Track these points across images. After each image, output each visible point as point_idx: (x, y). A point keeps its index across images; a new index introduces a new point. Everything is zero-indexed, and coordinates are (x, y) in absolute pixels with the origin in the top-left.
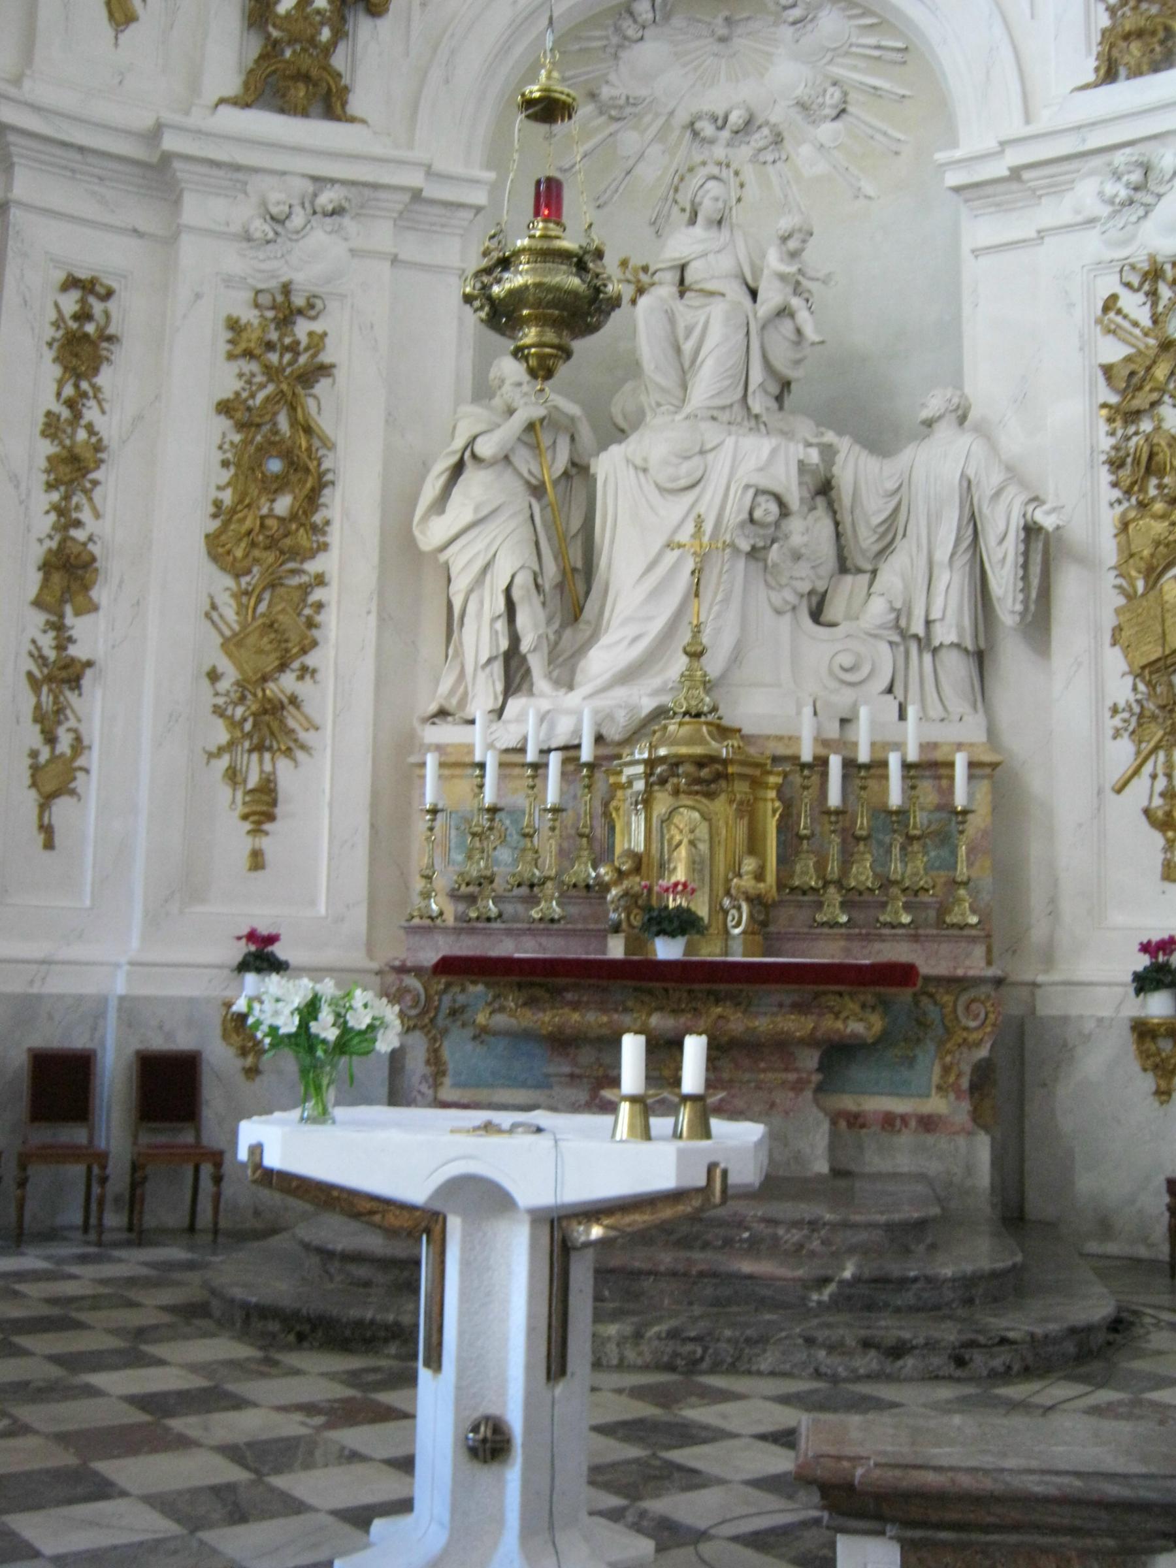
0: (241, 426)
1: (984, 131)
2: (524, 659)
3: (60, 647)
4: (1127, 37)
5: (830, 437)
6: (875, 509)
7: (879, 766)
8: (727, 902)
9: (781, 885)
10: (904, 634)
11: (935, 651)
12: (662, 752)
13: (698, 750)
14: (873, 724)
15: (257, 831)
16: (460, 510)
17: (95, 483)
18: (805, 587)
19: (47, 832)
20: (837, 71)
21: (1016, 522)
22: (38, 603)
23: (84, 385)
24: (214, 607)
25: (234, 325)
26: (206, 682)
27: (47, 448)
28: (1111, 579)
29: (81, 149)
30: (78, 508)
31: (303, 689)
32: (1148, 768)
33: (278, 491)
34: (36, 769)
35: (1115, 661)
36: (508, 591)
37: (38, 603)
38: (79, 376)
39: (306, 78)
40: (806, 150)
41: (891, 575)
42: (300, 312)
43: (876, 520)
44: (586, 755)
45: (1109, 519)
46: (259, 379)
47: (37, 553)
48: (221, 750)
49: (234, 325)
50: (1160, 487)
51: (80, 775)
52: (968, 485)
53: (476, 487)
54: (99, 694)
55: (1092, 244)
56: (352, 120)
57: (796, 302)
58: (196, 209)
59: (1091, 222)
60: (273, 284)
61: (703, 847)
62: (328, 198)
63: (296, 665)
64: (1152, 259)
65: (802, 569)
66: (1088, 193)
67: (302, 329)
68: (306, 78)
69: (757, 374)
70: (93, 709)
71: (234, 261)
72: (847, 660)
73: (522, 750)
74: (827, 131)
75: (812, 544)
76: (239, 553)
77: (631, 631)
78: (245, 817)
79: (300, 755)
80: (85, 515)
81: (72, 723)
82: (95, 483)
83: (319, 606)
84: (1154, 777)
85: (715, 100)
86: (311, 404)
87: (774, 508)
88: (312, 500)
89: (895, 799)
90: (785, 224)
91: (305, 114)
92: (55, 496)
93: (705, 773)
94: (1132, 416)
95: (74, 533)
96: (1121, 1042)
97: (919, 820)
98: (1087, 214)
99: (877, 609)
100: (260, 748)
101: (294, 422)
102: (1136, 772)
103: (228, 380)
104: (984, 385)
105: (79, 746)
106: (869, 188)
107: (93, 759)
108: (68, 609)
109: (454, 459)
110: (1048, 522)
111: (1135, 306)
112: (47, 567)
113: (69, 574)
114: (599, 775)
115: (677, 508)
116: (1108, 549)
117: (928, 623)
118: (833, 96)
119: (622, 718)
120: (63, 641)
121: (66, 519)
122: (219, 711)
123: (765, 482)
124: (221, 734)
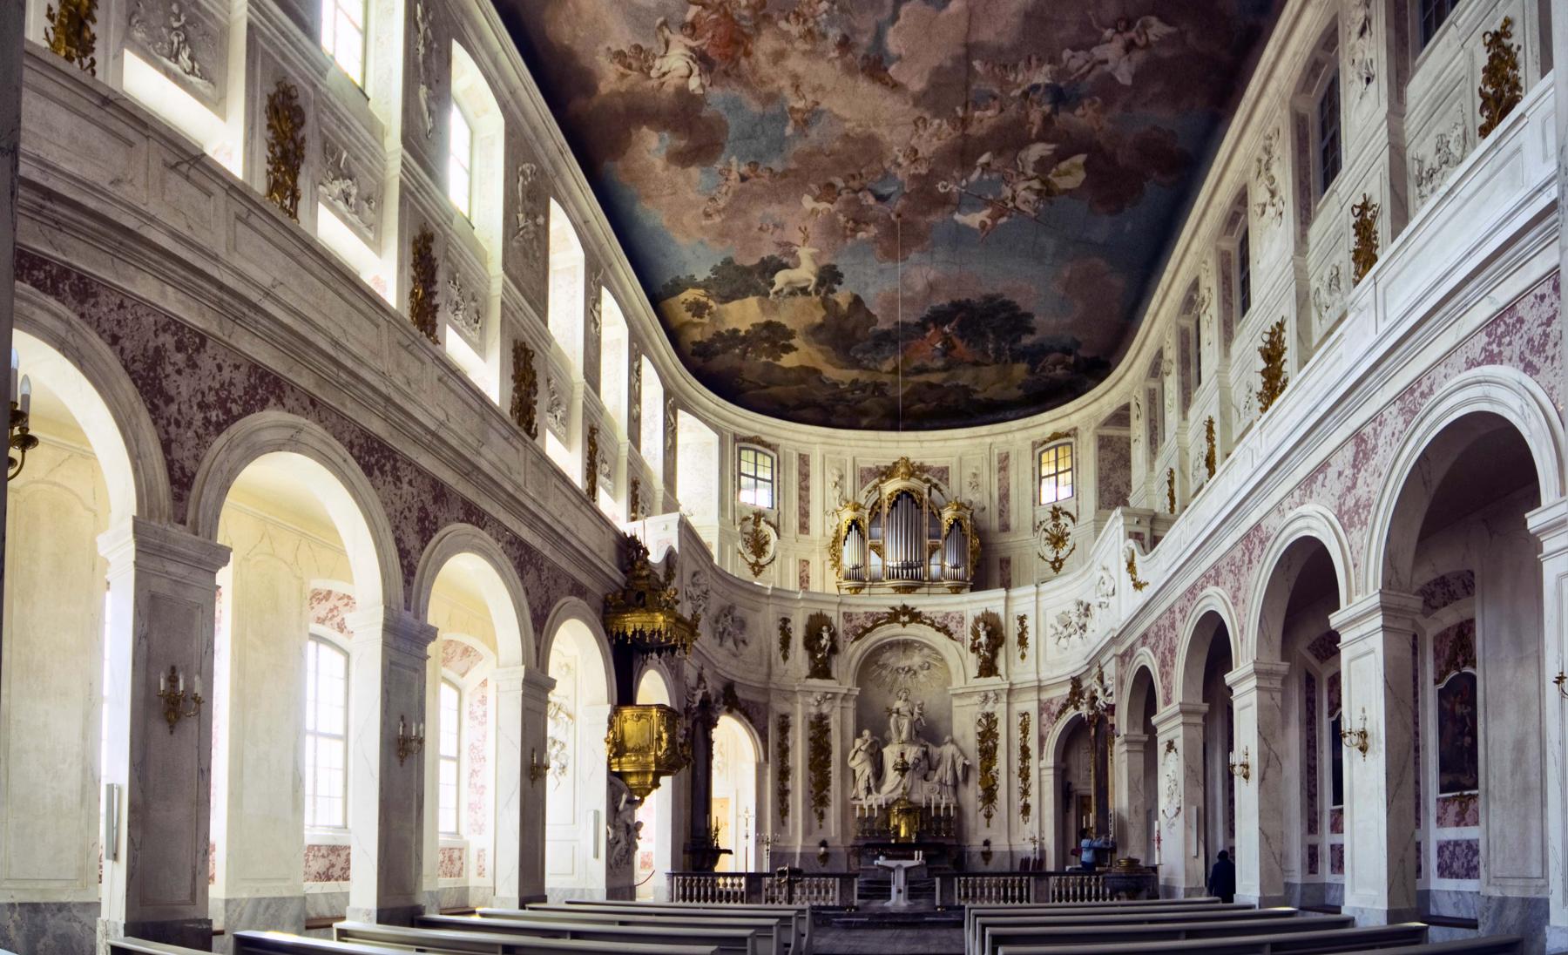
6: (936, 758)
53: (860, 755)
85: (901, 664)
104: (957, 733)
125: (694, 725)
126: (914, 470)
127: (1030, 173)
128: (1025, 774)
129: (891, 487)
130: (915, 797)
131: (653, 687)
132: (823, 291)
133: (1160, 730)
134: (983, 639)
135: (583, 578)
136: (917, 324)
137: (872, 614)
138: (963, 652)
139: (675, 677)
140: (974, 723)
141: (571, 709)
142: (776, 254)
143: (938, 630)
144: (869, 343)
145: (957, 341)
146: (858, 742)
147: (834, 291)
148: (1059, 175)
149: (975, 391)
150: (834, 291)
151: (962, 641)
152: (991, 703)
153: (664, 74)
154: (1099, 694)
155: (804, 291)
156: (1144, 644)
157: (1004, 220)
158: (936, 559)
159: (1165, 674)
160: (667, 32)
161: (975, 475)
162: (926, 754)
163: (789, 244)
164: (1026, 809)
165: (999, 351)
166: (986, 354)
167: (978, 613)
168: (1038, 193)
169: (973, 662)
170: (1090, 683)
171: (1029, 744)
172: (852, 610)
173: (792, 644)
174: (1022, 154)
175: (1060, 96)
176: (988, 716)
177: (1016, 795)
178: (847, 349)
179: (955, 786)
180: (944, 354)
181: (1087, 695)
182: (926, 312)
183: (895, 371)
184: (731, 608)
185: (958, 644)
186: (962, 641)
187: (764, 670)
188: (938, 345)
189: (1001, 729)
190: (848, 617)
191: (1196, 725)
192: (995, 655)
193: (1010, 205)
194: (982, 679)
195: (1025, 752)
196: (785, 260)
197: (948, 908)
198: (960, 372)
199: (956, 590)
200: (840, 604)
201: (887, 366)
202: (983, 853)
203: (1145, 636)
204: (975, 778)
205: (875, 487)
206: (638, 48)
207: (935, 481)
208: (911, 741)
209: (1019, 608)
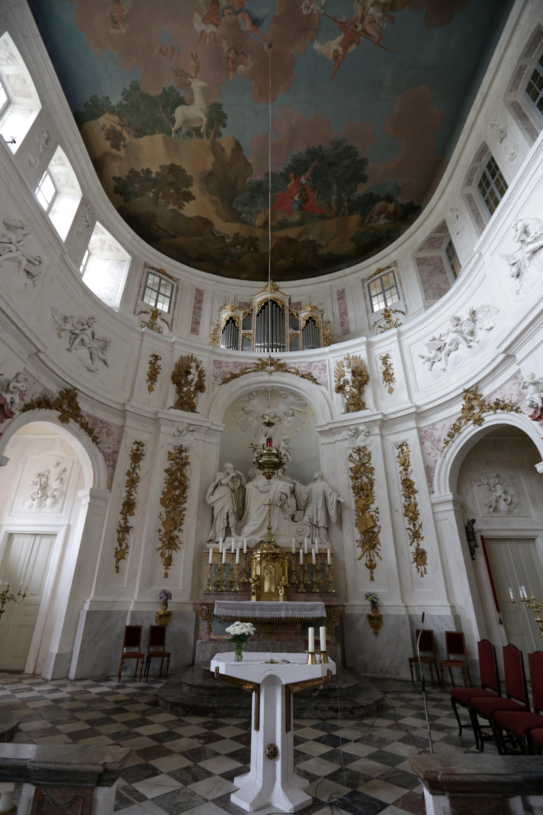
0: (169, 475)
1: (323, 420)
2: (230, 528)
3: (125, 523)
4: (351, 404)
5: (294, 481)
7: (310, 554)
8: (279, 587)
9: (289, 582)
10: (311, 524)
11: (319, 528)
12: (264, 552)
13: (272, 551)
14: (308, 545)
15: (167, 568)
17: (137, 486)
18: (291, 514)
19: (117, 568)
21: (335, 500)
22: (121, 513)
23: (136, 465)
24: (161, 515)
25: (170, 453)
26: (158, 532)
27: (127, 478)
28: (354, 512)
29: (141, 415)
30: (132, 492)
31: (180, 534)
32: (365, 554)
33: (177, 489)
34: (116, 553)
35: (356, 530)
36: (227, 514)
37: (121, 513)
38: (135, 463)
39: (188, 404)
40: (286, 422)
41: (309, 511)
42: (184, 451)
43: (304, 499)
44: (245, 551)
45: (353, 500)
46: (174, 465)
47: (122, 501)
48: (160, 548)
49: (170, 453)
50: (363, 493)
51: (127, 554)
52: (324, 492)
54: (133, 534)
55: (346, 444)
56: (197, 412)
57: (287, 453)
58: (163, 429)
59: (346, 439)
60: (178, 445)
61: (274, 574)
62: (191, 428)
63: (178, 529)
64: (359, 447)
65: (290, 510)
66: (345, 434)
67: (184, 454)
68: (188, 404)
70: (131, 538)
71: (171, 440)
72: (300, 530)
73: (230, 550)
74: (290, 418)
75: (295, 505)
76: (167, 503)
77: (254, 523)
78: (164, 565)
79: (178, 550)
80: (134, 493)
81: (126, 541)
82: (137, 486)
83: (184, 515)
84: (367, 556)
86: (185, 470)
87: (285, 497)
88: (184, 492)
89: (314, 562)
90: (285, 437)
91: (187, 411)
92: (128, 489)
93: (274, 557)
94: (357, 479)
95: (131, 497)
97: (318, 567)
98: (345, 438)
99: (306, 519)
101: (181, 474)
102: (363, 555)
103: (167, 465)
105: (127, 547)
106: (298, 430)
107: (130, 550)
108: (128, 514)
109: (216, 484)
110: (342, 501)
111: (355, 456)
112: (124, 505)
113: (129, 506)
114: (248, 556)
115: (264, 496)
116: (353, 506)
117: (317, 522)
118: (291, 412)
119: (253, 543)
120: (126, 522)
121: (129, 494)
122: (160, 539)
123: (283, 491)
124: (160, 545)
128: (411, 512)
134: (348, 376)
137: (240, 364)
138: (328, 394)
143: (303, 376)
152: (362, 437)
164: (420, 556)
169: (338, 401)
171: (412, 478)
172: (223, 359)
173: (159, 378)
176: (359, 450)
185: (323, 388)
189: (376, 462)
190: (218, 364)
192: (361, 392)
195: (408, 486)
204: (350, 518)
209: (379, 351)
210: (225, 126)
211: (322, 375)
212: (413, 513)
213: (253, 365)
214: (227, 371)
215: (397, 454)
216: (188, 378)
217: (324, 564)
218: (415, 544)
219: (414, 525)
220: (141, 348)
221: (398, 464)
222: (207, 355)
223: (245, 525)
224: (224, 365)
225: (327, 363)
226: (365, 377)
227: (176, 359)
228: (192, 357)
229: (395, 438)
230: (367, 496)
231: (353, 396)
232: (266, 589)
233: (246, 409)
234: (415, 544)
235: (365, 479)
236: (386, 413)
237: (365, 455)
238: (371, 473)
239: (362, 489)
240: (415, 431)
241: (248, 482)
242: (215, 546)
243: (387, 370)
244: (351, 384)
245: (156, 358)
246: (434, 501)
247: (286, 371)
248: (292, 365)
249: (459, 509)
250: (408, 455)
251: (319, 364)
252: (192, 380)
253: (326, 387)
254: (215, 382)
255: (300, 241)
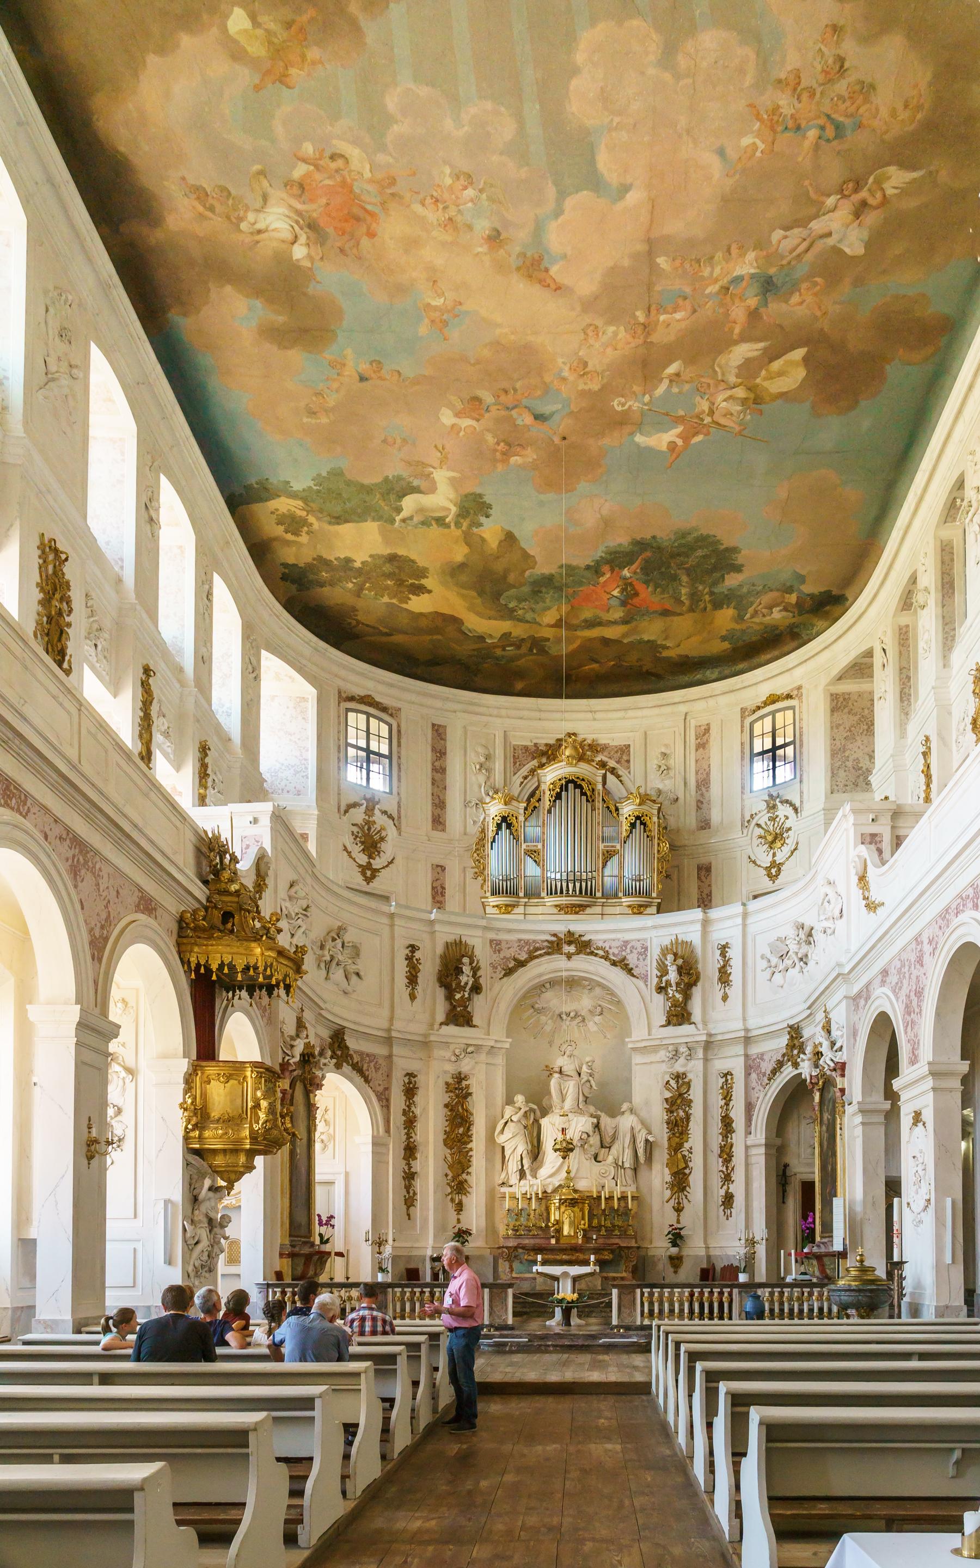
0: (451, 1110)
5: (599, 1113)
16: (508, 1133)
20: (600, 1003)
25: (447, 1083)
35: (667, 1171)
40: (591, 1023)
45: (666, 1136)
49: (447, 1083)
52: (632, 1128)
53: (511, 1129)
56: (474, 1026)
58: (438, 1053)
62: (470, 1050)
65: (593, 1149)
66: (662, 1055)
67: (464, 1083)
68: (463, 1016)
69: (581, 1098)
74: (597, 1019)
80: (413, 1135)
85: (565, 1009)
88: (469, 1129)
90: (588, 1059)
94: (672, 1112)
96: (667, 1261)
99: (610, 1159)
100: (458, 1193)
110: (651, 1139)
118: (599, 1009)
125: (292, 1085)
126: (586, 751)
127: (732, 379)
128: (726, 1154)
129: (552, 774)
130: (582, 1185)
131: (241, 1037)
132: (465, 524)
133: (903, 1097)
134: (673, 976)
135: (150, 887)
136: (588, 568)
137: (527, 942)
139: (267, 1024)
140: (661, 1084)
141: (130, 1063)
142: (405, 474)
143: (614, 964)
144: (526, 589)
145: (640, 587)
146: (509, 1111)
147: (481, 525)
148: (770, 378)
149: (665, 648)
150: (481, 525)
151: (645, 978)
152: (682, 1060)
153: (259, 232)
154: (825, 1049)
155: (440, 521)
156: (883, 983)
157: (699, 438)
158: (612, 868)
159: (911, 1025)
160: (265, 183)
161: (664, 755)
162: (597, 1126)
163: (424, 465)
164: (728, 1200)
165: (695, 597)
166: (679, 601)
167: (666, 942)
168: (744, 402)
169: (659, 1006)
170: (813, 1033)
171: (732, 1115)
172: (503, 936)
174: (722, 359)
175: (767, 286)
176: (678, 1077)
177: (716, 1180)
178: (497, 596)
179: (635, 1170)
180: (624, 603)
181: (809, 1050)
182: (599, 553)
183: (558, 624)
184: (340, 931)
185: (640, 983)
186: (645, 978)
187: (386, 1013)
188: (615, 593)
189: (696, 1094)
190: (496, 945)
191: (951, 1090)
192: (687, 997)
193: (708, 420)
194: (672, 1030)
196: (416, 483)
197: (628, 1328)
198: (644, 624)
199: (639, 910)
200: (485, 928)
201: (550, 617)
202: (671, 1258)
203: (885, 972)
205: (533, 771)
206: (223, 189)
207: (612, 763)
208: (578, 1111)
209: (720, 934)
210: (487, 517)
211: (641, 963)
212: (728, 1155)
213: (546, 944)
214: (508, 956)
215: (720, 1085)
216: (460, 982)
217: (627, 1206)
218: (725, 1187)
219: (727, 1167)
220: (392, 938)
221: (721, 1097)
222: (479, 933)
223: (540, 1167)
224: (504, 945)
225: (649, 945)
226: (694, 977)
227: (440, 950)
228: (461, 942)
229: (720, 1065)
230: (681, 1134)
231: (675, 1004)
232: (565, 1233)
233: (537, 1006)
234: (725, 1187)
235: (681, 1113)
236: (713, 1032)
237: (684, 1083)
238: (690, 1106)
239: (676, 1125)
240: (742, 1058)
241: (543, 1117)
242: (511, 1190)
243: (724, 966)
244: (674, 988)
245: (413, 948)
246: (749, 1143)
247: (592, 953)
248: (600, 944)
249: (773, 1151)
250: (732, 1088)
251: (638, 945)
252: (466, 984)
253: (646, 982)
254: (494, 975)
255: (625, 641)
